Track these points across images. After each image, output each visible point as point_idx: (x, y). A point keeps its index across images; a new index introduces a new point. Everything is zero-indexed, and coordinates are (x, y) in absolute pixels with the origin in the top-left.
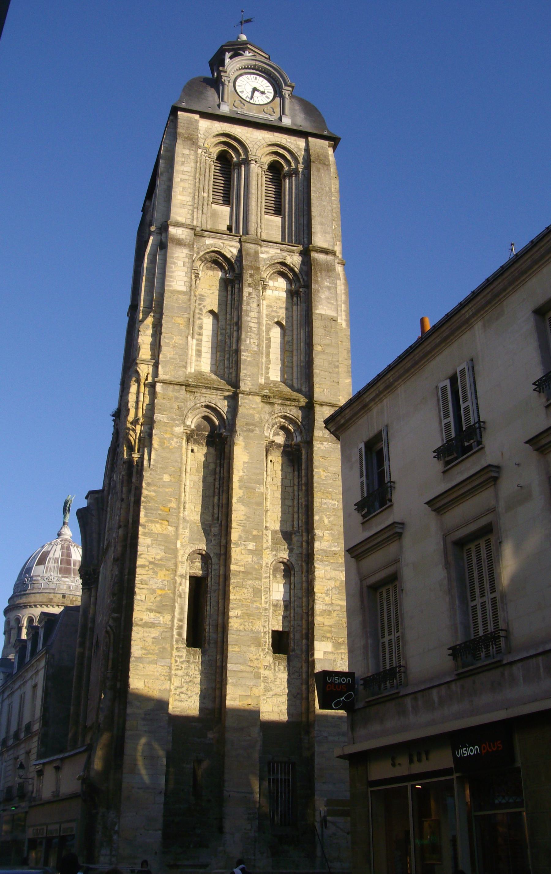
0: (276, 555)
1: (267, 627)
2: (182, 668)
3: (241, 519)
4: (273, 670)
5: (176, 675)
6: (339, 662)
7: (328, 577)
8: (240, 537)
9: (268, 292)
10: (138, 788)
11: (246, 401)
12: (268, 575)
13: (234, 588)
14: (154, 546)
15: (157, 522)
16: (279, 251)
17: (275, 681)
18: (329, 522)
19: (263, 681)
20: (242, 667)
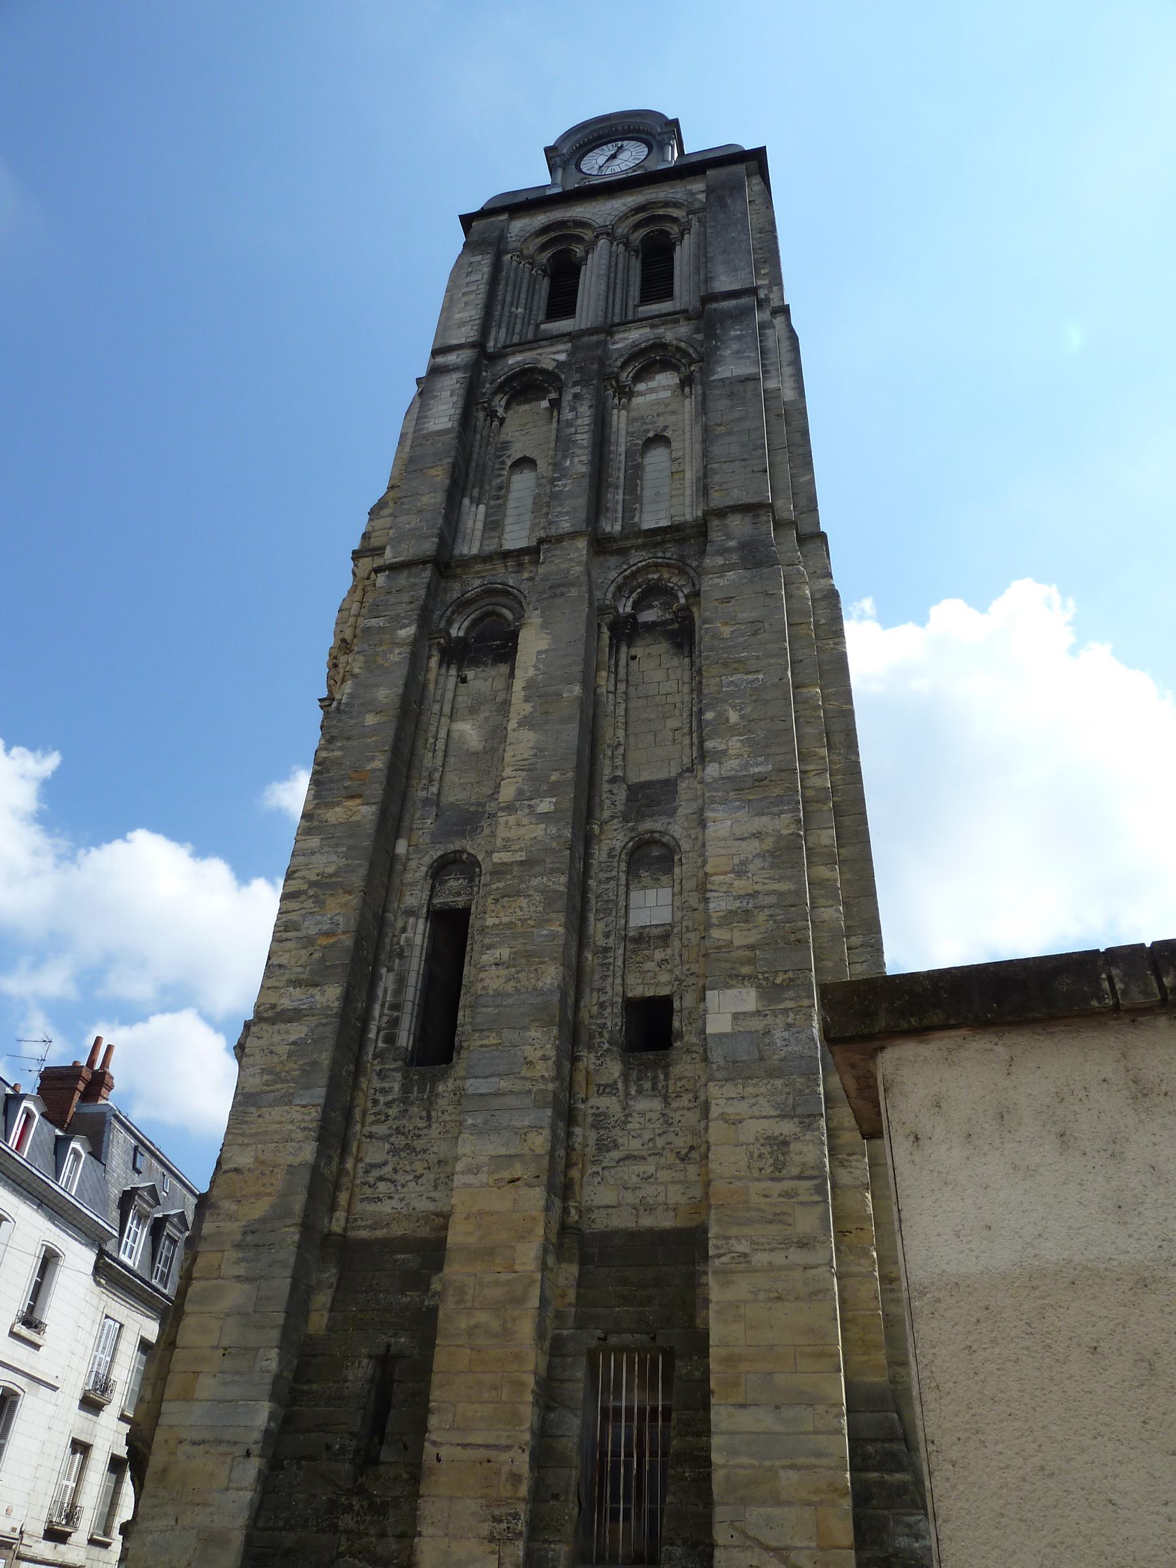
0: (633, 829)
2: (387, 1116)
4: (621, 1093)
5: (371, 1136)
6: (778, 1035)
7: (739, 834)
8: (520, 792)
9: (637, 401)
10: (194, 1443)
11: (556, 552)
12: (614, 873)
13: (497, 900)
14: (326, 849)
15: (338, 804)
16: (648, 330)
17: (625, 1123)
18: (742, 717)
19: (593, 1126)
20: (503, 1084)
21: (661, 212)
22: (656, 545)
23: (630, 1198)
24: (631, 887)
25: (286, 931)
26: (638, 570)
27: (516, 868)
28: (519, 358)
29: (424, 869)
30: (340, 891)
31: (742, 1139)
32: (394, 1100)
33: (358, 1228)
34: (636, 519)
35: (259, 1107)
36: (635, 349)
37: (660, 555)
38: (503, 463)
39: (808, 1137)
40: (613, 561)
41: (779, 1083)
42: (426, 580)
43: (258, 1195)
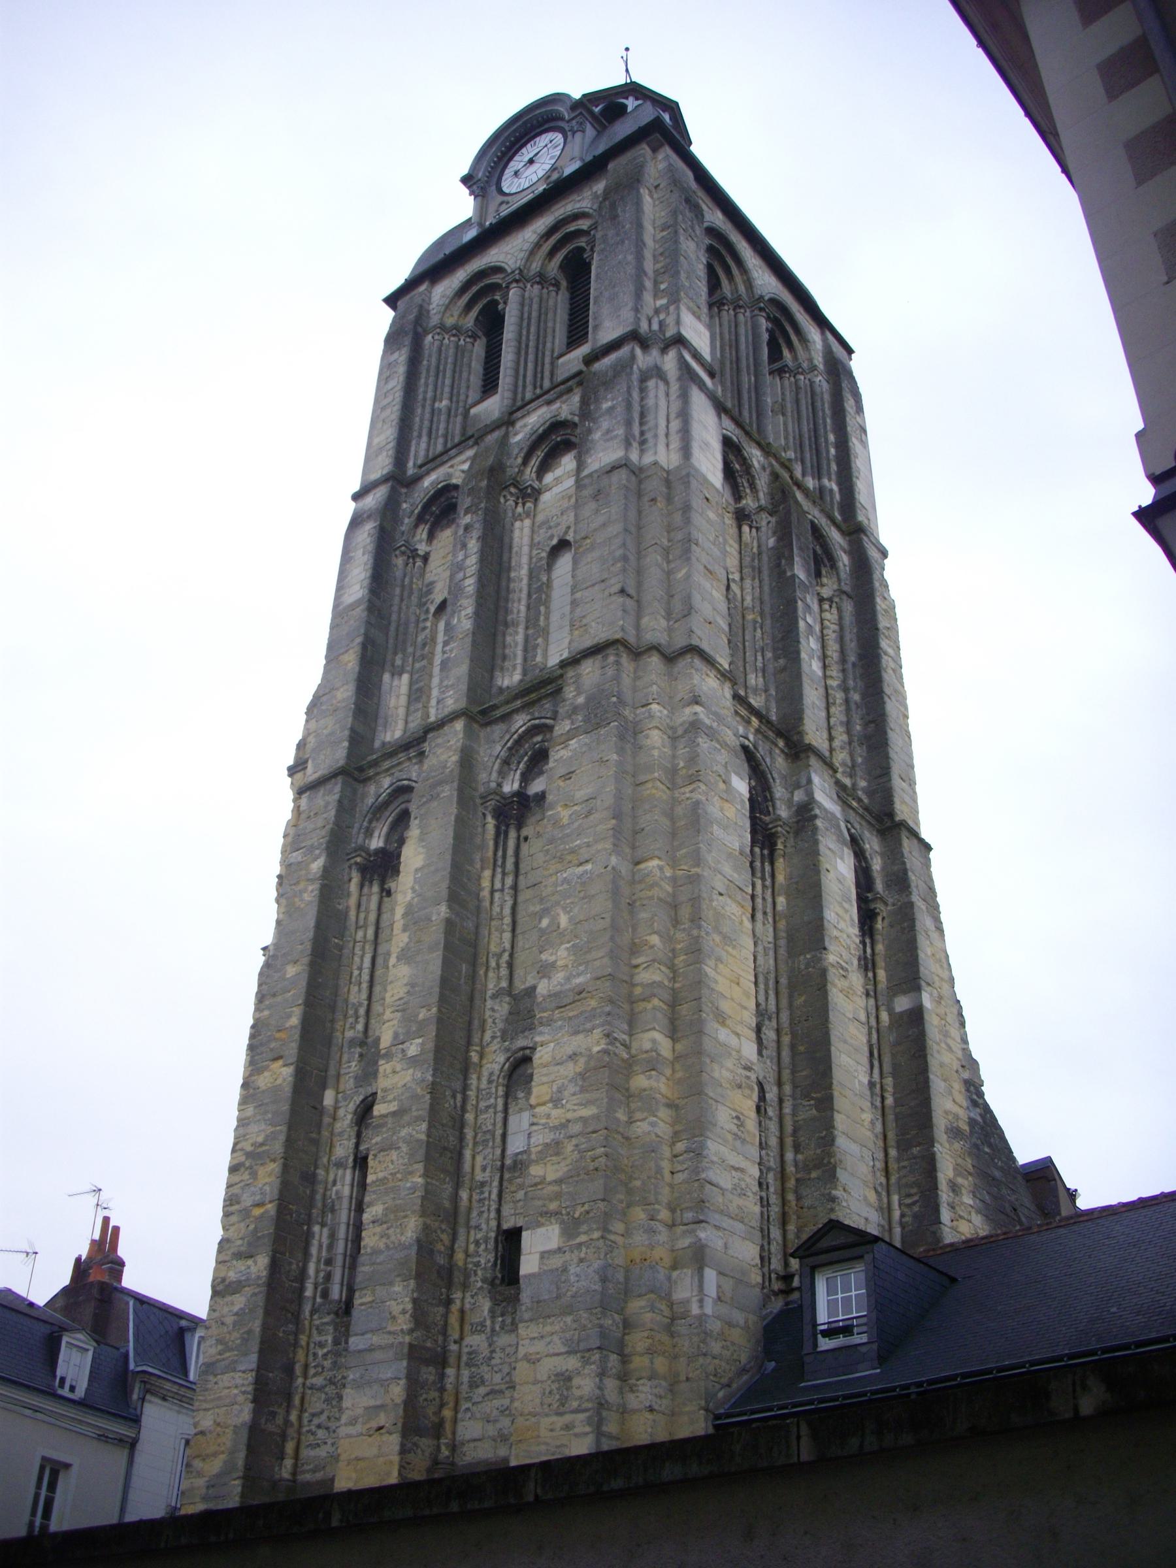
1: (484, 1226)
3: (401, 995)
4: (488, 1329)
6: (572, 1271)
8: (396, 1035)
9: (546, 497)
12: (492, 1101)
16: (544, 409)
17: (491, 1358)
19: (467, 1364)
20: (376, 1339)
21: (572, 227)
22: (532, 704)
23: (491, 1430)
24: (510, 1111)
25: (231, 1205)
26: (521, 737)
27: (390, 1120)
28: (433, 477)
29: (349, 1117)
30: (268, 1161)
31: (539, 1377)
32: (328, 1352)
33: (304, 1472)
34: (539, 659)
35: (215, 1375)
36: (534, 437)
37: (537, 715)
38: (427, 611)
39: (586, 1371)
40: (498, 729)
41: (569, 1319)
42: (337, 797)
43: (215, 1454)
